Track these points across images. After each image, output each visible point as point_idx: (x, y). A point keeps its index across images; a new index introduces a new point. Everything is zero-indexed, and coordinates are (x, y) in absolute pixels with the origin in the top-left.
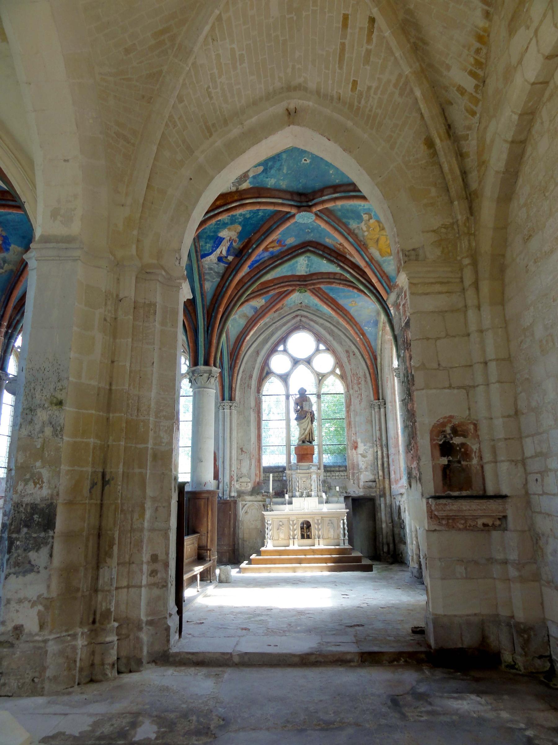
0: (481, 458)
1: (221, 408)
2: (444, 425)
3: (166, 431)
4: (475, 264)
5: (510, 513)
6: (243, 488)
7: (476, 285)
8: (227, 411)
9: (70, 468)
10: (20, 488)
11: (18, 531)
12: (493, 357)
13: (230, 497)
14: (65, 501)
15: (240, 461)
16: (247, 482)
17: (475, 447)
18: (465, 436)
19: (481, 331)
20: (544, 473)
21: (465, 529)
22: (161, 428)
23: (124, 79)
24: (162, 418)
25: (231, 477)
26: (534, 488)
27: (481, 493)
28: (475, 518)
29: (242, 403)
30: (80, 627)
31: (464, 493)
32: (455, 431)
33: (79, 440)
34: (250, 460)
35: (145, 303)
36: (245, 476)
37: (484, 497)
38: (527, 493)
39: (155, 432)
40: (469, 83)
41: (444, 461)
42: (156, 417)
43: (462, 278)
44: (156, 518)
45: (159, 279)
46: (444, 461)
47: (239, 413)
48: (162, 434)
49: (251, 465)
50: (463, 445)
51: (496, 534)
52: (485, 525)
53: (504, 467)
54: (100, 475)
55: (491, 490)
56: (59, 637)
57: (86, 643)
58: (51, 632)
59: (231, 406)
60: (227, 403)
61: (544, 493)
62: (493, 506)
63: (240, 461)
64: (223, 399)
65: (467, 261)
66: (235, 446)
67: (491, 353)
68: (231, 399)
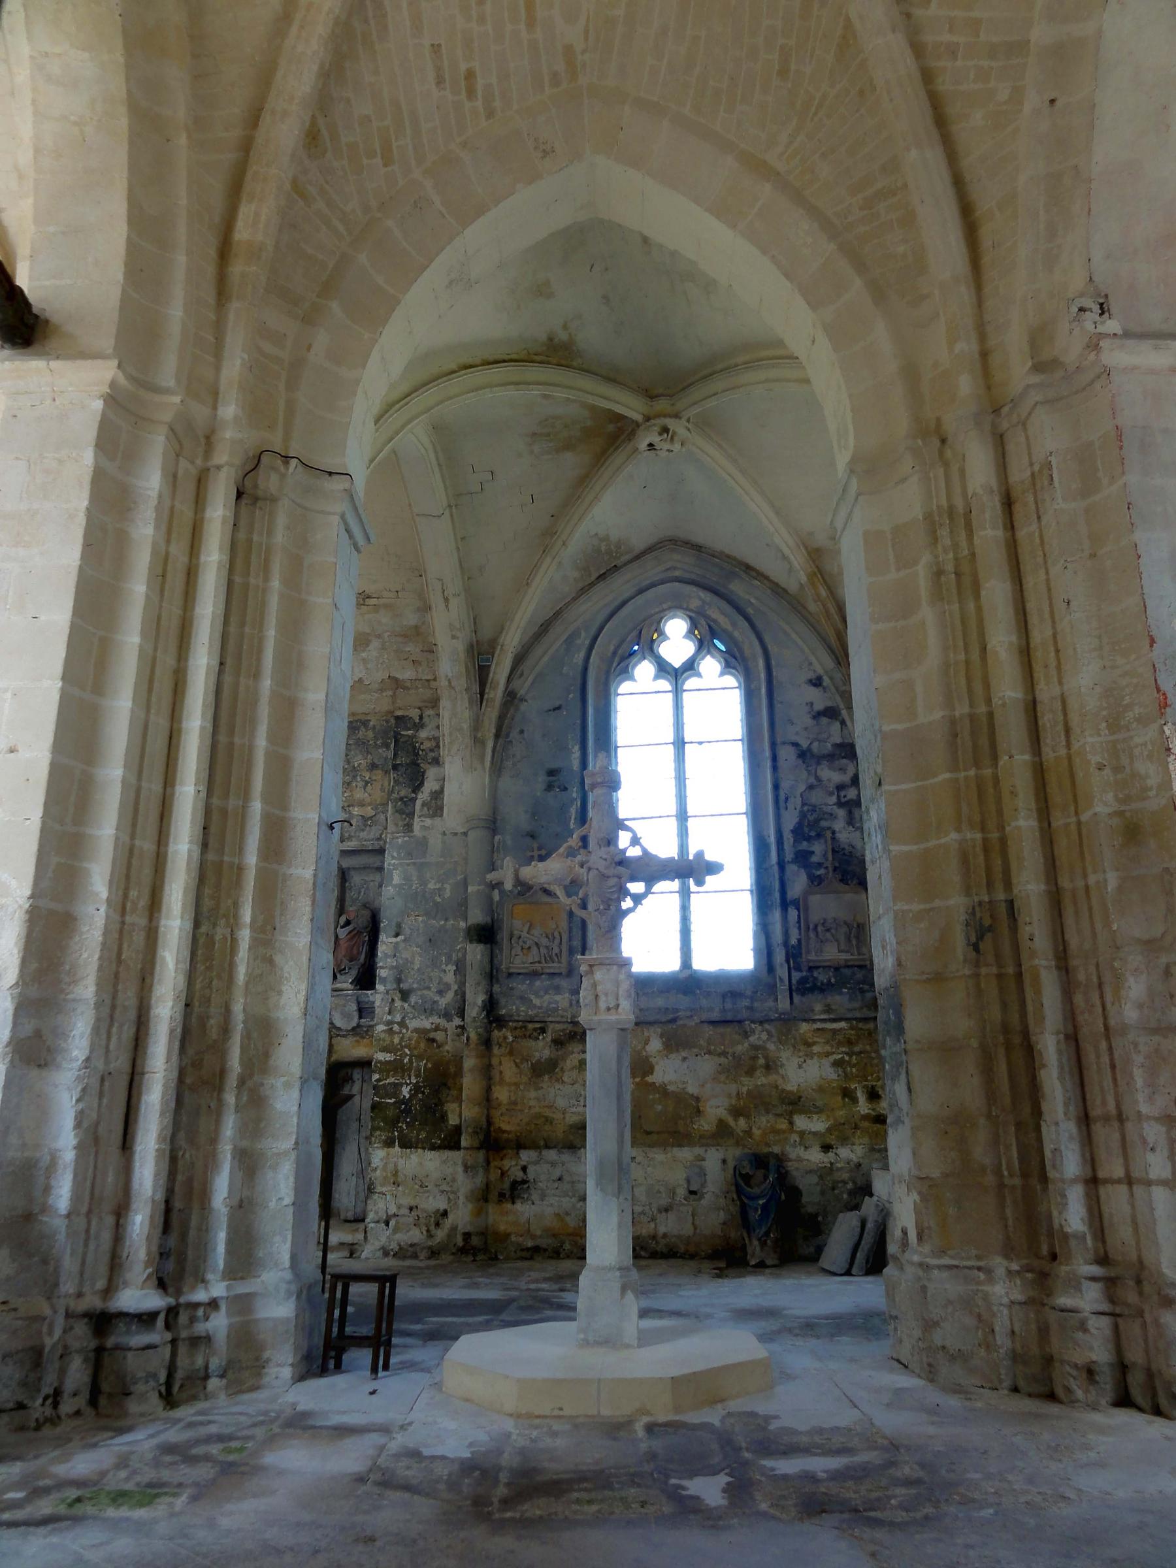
3: (1150, 757)
9: (916, 907)
14: (925, 977)
22: (1137, 751)
23: (816, 113)
24: (1134, 725)
30: (1007, 1257)
33: (932, 843)
35: (1033, 474)
39: (1117, 769)
42: (1114, 725)
44: (1172, 996)
45: (1038, 398)
48: (1142, 767)
54: (1002, 909)
56: (957, 1267)
57: (1018, 1296)
58: (942, 1252)
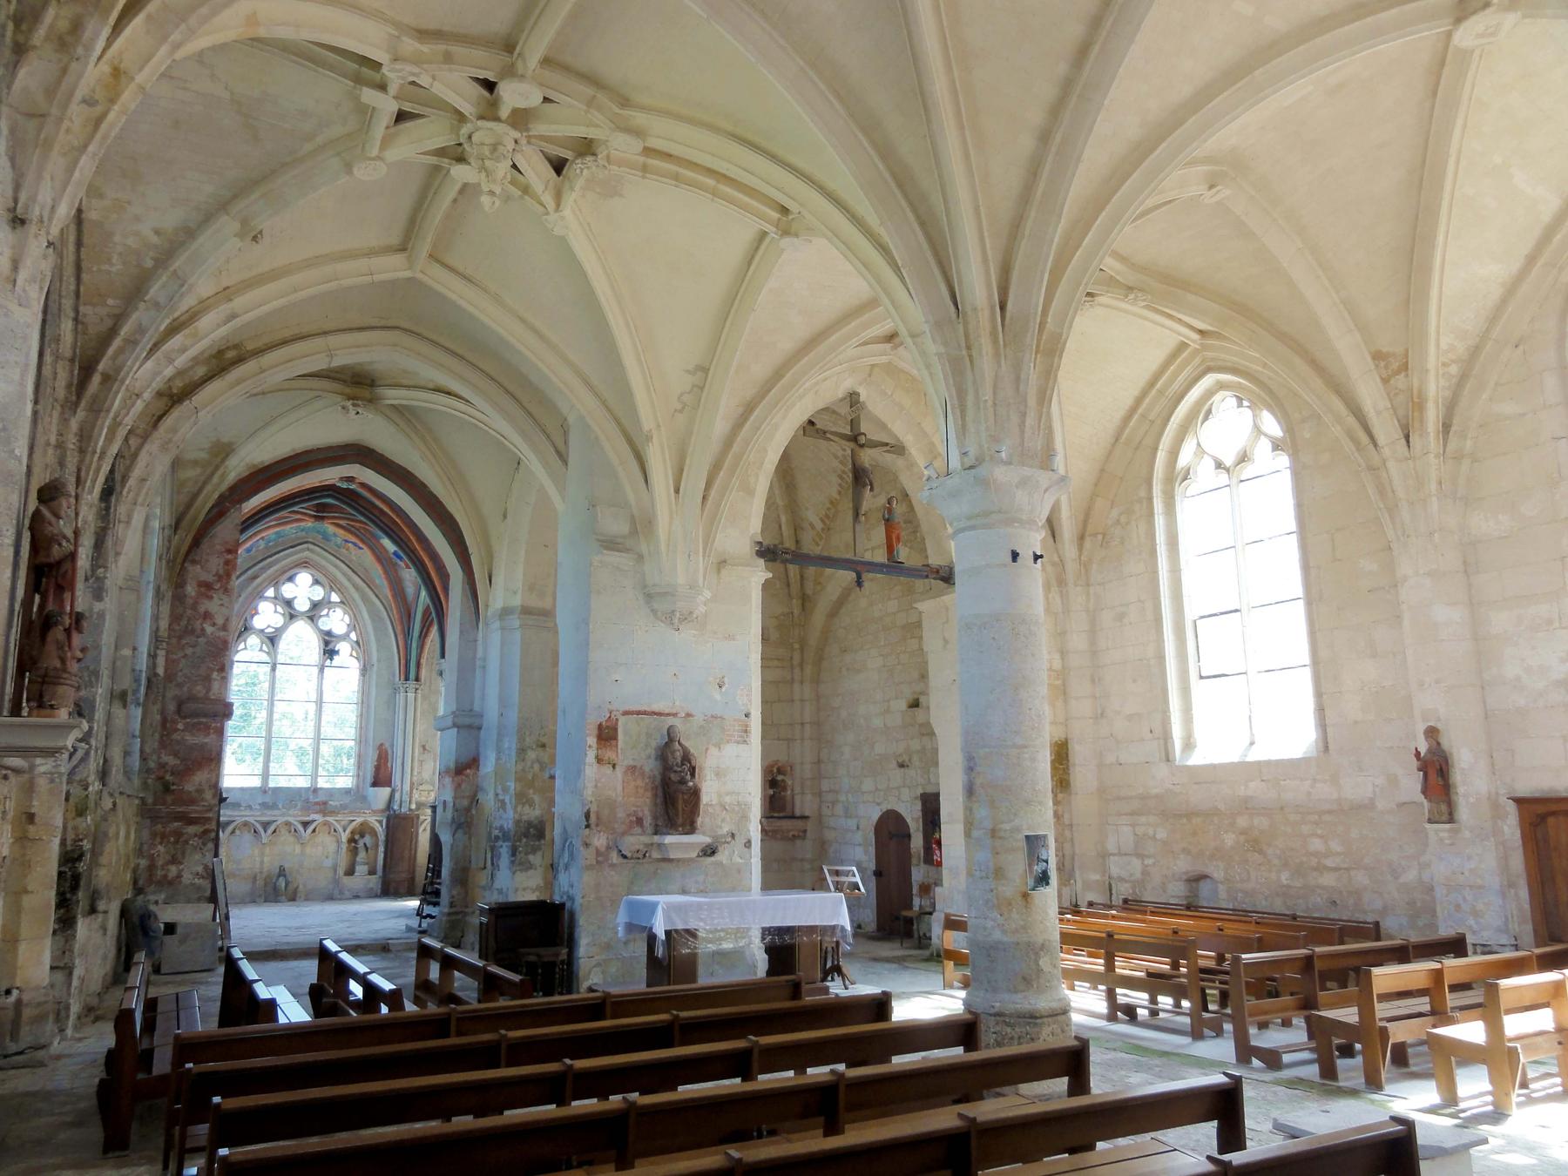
0: (792, 790)
1: (402, 690)
2: (772, 766)
4: (802, 649)
5: (809, 829)
6: (423, 799)
7: (801, 665)
8: (411, 695)
10: (519, 809)
11: (520, 841)
12: (809, 720)
13: (410, 810)
15: (421, 762)
16: (429, 791)
17: (790, 783)
18: (785, 775)
19: (802, 700)
20: (834, 803)
21: (782, 839)
25: (412, 784)
26: (825, 811)
27: (790, 814)
28: (789, 831)
29: (428, 684)
31: (781, 815)
32: (780, 771)
34: (435, 762)
36: (427, 782)
37: (793, 817)
38: (820, 815)
40: (819, 526)
41: (771, 792)
43: (791, 658)
46: (771, 792)
47: (424, 698)
49: (435, 766)
50: (783, 781)
51: (798, 842)
52: (794, 836)
53: (809, 797)
55: (798, 813)
59: (417, 689)
60: (412, 684)
61: (833, 815)
62: (799, 824)
63: (421, 762)
64: (407, 679)
65: (797, 646)
66: (417, 745)
67: (807, 718)
68: (417, 679)
